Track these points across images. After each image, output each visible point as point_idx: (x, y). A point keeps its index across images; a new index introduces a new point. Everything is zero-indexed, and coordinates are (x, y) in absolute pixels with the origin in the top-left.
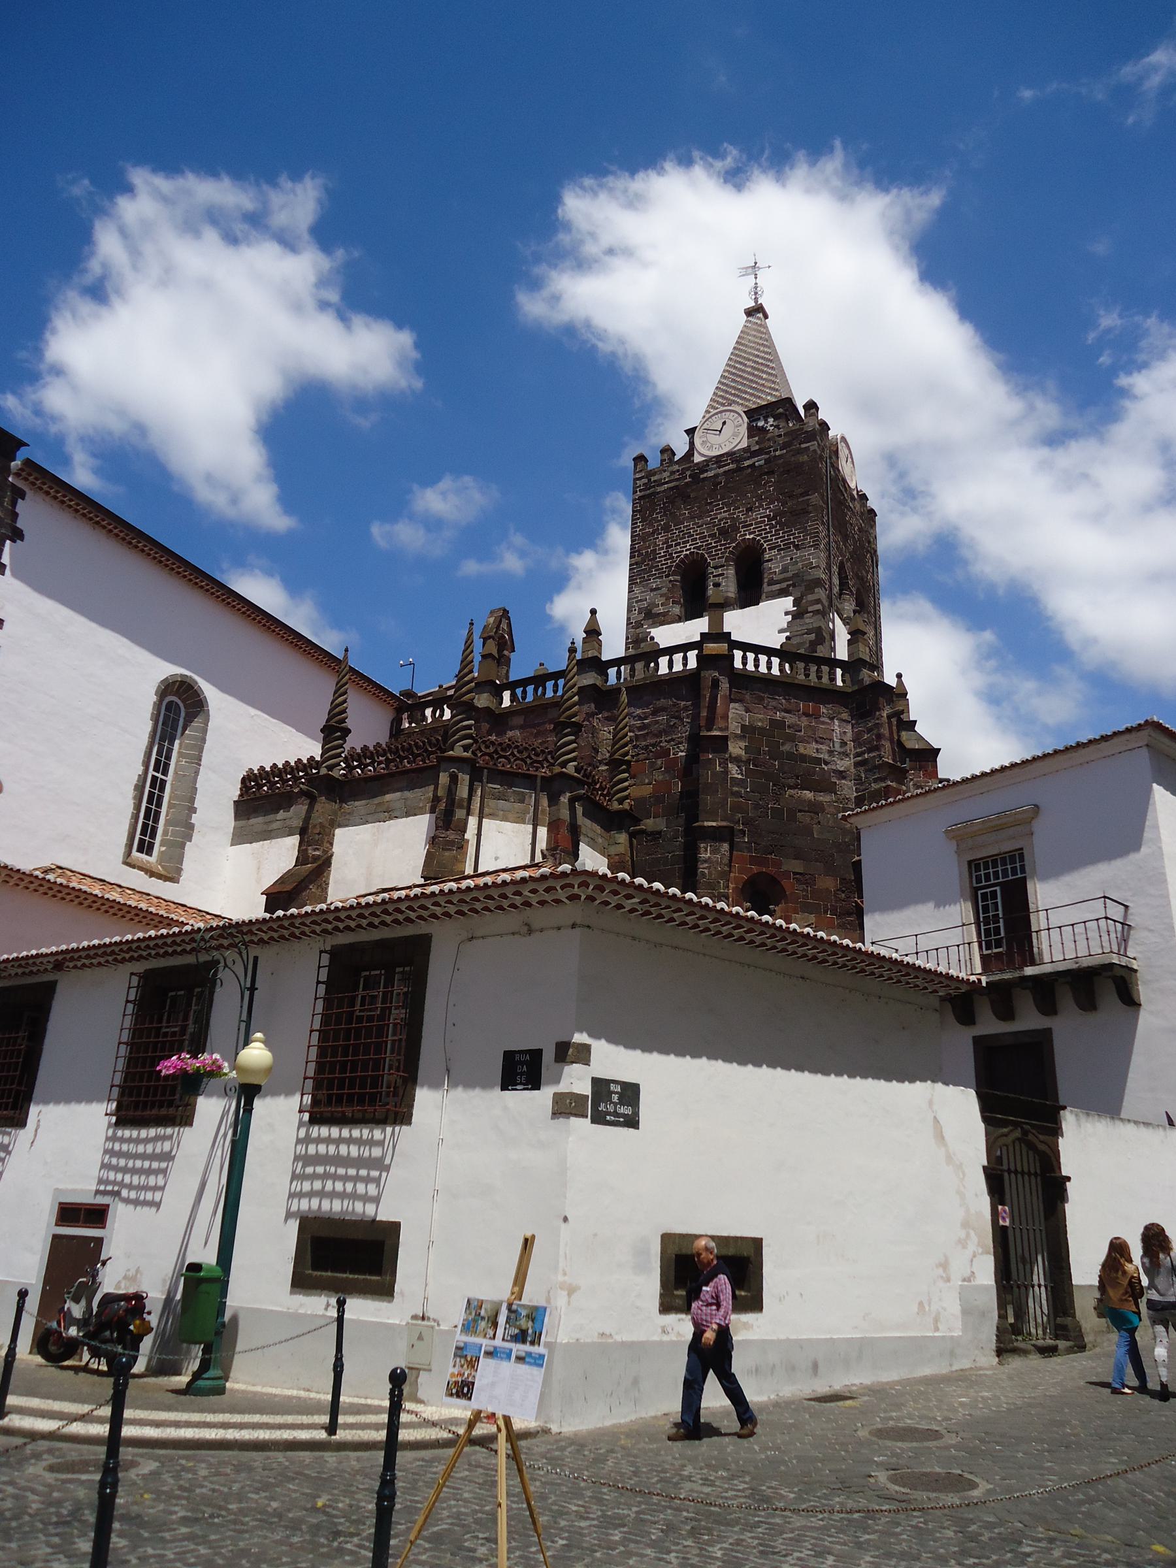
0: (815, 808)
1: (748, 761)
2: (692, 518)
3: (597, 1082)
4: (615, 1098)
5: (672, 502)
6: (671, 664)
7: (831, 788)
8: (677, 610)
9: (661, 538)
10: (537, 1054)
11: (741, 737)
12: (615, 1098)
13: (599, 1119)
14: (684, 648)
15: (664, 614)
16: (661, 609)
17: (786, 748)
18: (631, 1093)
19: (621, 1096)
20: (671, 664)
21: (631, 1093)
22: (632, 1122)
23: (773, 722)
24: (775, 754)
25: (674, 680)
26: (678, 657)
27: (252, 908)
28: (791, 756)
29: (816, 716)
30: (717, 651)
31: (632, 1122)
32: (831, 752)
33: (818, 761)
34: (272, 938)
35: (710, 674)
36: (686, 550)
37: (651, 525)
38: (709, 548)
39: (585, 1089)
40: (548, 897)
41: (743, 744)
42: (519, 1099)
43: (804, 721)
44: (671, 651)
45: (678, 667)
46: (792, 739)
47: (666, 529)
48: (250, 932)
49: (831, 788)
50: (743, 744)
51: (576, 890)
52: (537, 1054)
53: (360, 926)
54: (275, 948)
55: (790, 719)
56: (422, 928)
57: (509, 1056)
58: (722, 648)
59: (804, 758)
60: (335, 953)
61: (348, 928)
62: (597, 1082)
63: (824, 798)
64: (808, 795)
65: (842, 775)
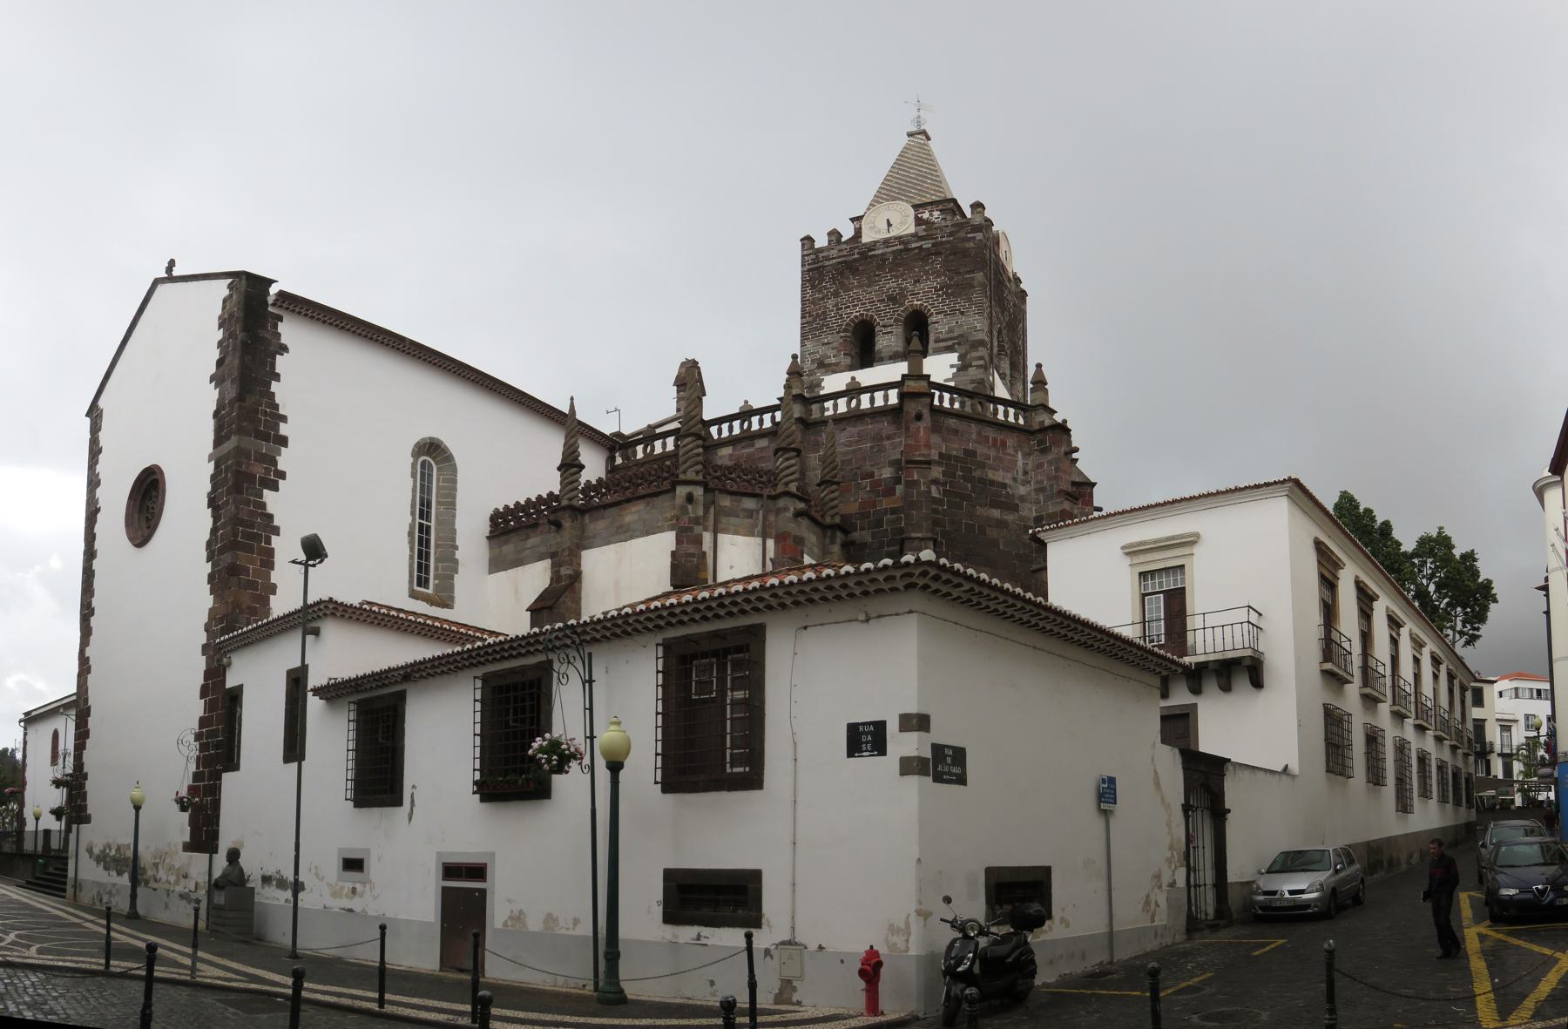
0: (1001, 524)
1: (944, 484)
2: (860, 286)
3: (937, 749)
4: (949, 760)
5: (841, 274)
6: (872, 400)
7: (1015, 508)
8: (848, 360)
9: (831, 303)
10: (880, 726)
11: (939, 463)
12: (949, 760)
13: (938, 779)
14: (886, 387)
15: (837, 364)
16: (833, 360)
17: (977, 474)
18: (959, 755)
19: (953, 758)
20: (872, 400)
21: (959, 755)
22: (961, 780)
23: (966, 451)
24: (968, 478)
25: (875, 413)
26: (879, 395)
27: (518, 624)
28: (983, 481)
29: (1004, 444)
30: (915, 389)
31: (961, 780)
32: (1015, 479)
33: (1004, 486)
34: (604, 637)
35: (912, 407)
36: (857, 312)
37: (820, 291)
38: (878, 311)
39: (927, 753)
40: (886, 587)
41: (941, 469)
42: (867, 764)
43: (992, 453)
44: (872, 389)
45: (879, 402)
46: (982, 466)
47: (836, 294)
48: (585, 632)
49: (1015, 508)
50: (941, 469)
51: (913, 580)
52: (880, 726)
53: (693, 620)
54: (605, 646)
55: (981, 450)
56: (754, 619)
57: (853, 730)
58: (919, 386)
59: (992, 483)
60: (667, 646)
61: (681, 623)
62: (937, 749)
63: (1009, 517)
64: (996, 513)
65: (1023, 499)
